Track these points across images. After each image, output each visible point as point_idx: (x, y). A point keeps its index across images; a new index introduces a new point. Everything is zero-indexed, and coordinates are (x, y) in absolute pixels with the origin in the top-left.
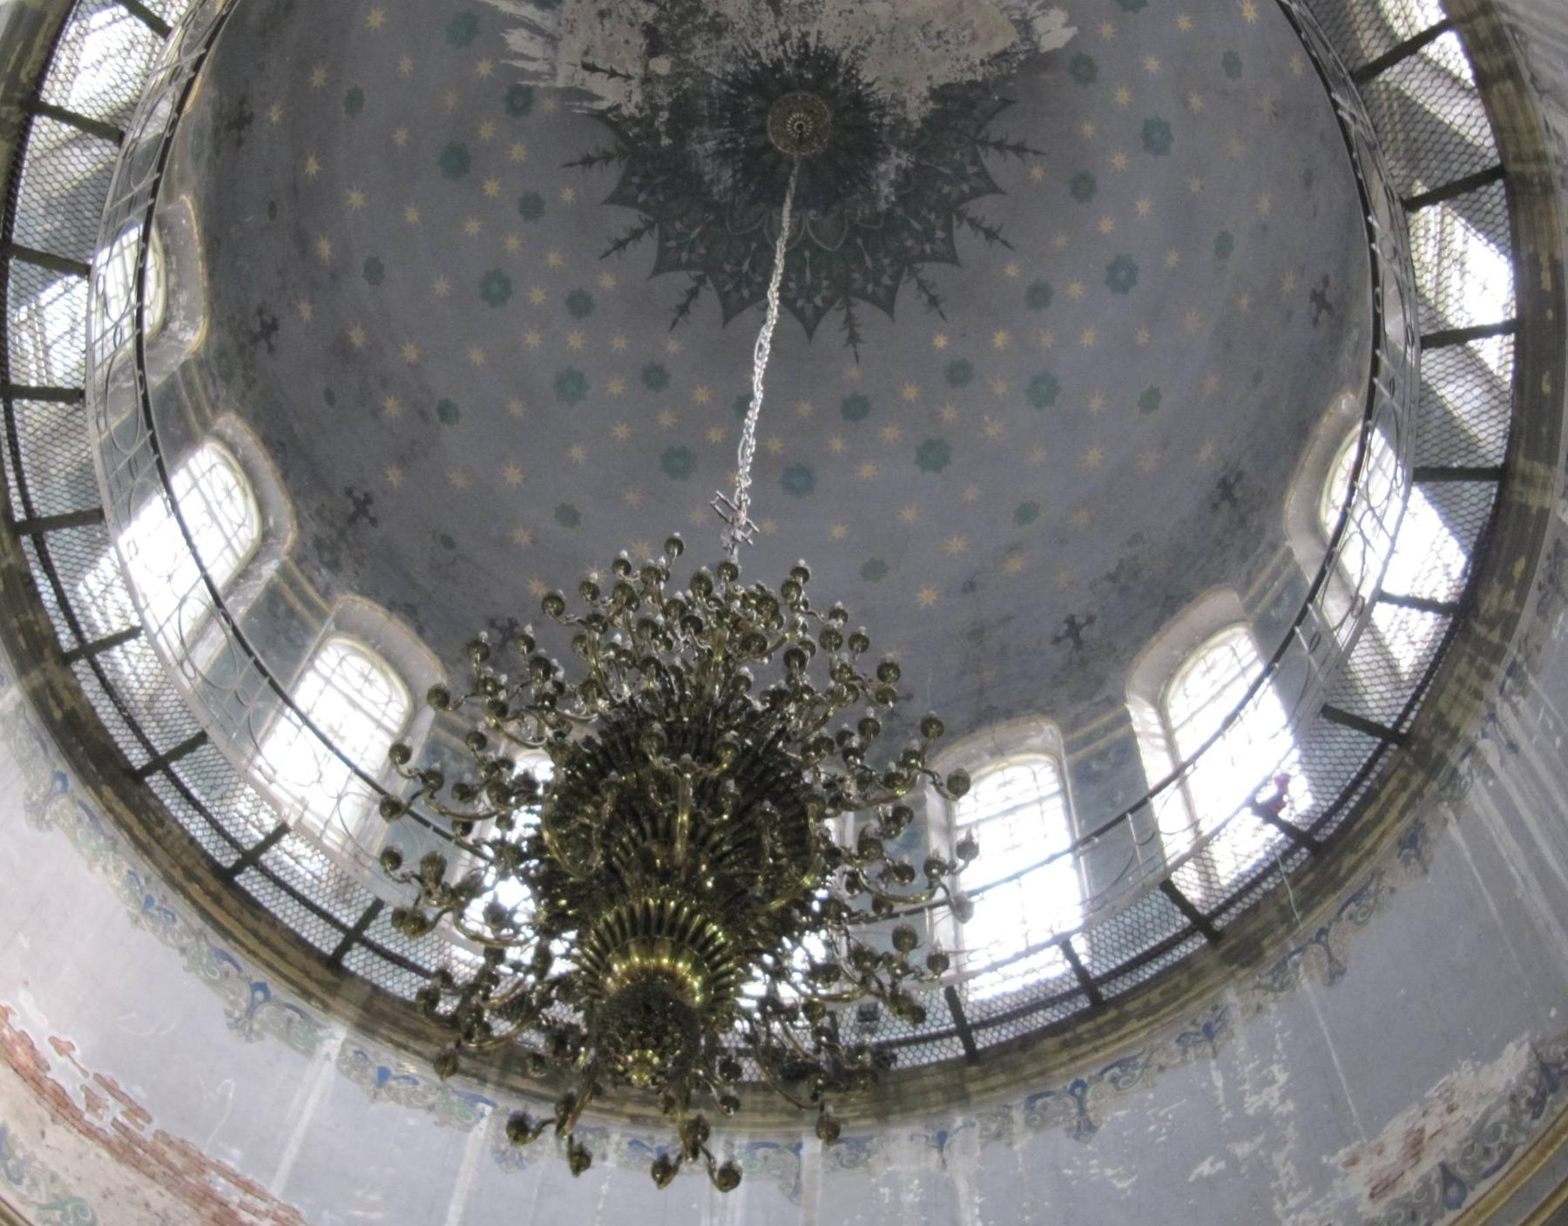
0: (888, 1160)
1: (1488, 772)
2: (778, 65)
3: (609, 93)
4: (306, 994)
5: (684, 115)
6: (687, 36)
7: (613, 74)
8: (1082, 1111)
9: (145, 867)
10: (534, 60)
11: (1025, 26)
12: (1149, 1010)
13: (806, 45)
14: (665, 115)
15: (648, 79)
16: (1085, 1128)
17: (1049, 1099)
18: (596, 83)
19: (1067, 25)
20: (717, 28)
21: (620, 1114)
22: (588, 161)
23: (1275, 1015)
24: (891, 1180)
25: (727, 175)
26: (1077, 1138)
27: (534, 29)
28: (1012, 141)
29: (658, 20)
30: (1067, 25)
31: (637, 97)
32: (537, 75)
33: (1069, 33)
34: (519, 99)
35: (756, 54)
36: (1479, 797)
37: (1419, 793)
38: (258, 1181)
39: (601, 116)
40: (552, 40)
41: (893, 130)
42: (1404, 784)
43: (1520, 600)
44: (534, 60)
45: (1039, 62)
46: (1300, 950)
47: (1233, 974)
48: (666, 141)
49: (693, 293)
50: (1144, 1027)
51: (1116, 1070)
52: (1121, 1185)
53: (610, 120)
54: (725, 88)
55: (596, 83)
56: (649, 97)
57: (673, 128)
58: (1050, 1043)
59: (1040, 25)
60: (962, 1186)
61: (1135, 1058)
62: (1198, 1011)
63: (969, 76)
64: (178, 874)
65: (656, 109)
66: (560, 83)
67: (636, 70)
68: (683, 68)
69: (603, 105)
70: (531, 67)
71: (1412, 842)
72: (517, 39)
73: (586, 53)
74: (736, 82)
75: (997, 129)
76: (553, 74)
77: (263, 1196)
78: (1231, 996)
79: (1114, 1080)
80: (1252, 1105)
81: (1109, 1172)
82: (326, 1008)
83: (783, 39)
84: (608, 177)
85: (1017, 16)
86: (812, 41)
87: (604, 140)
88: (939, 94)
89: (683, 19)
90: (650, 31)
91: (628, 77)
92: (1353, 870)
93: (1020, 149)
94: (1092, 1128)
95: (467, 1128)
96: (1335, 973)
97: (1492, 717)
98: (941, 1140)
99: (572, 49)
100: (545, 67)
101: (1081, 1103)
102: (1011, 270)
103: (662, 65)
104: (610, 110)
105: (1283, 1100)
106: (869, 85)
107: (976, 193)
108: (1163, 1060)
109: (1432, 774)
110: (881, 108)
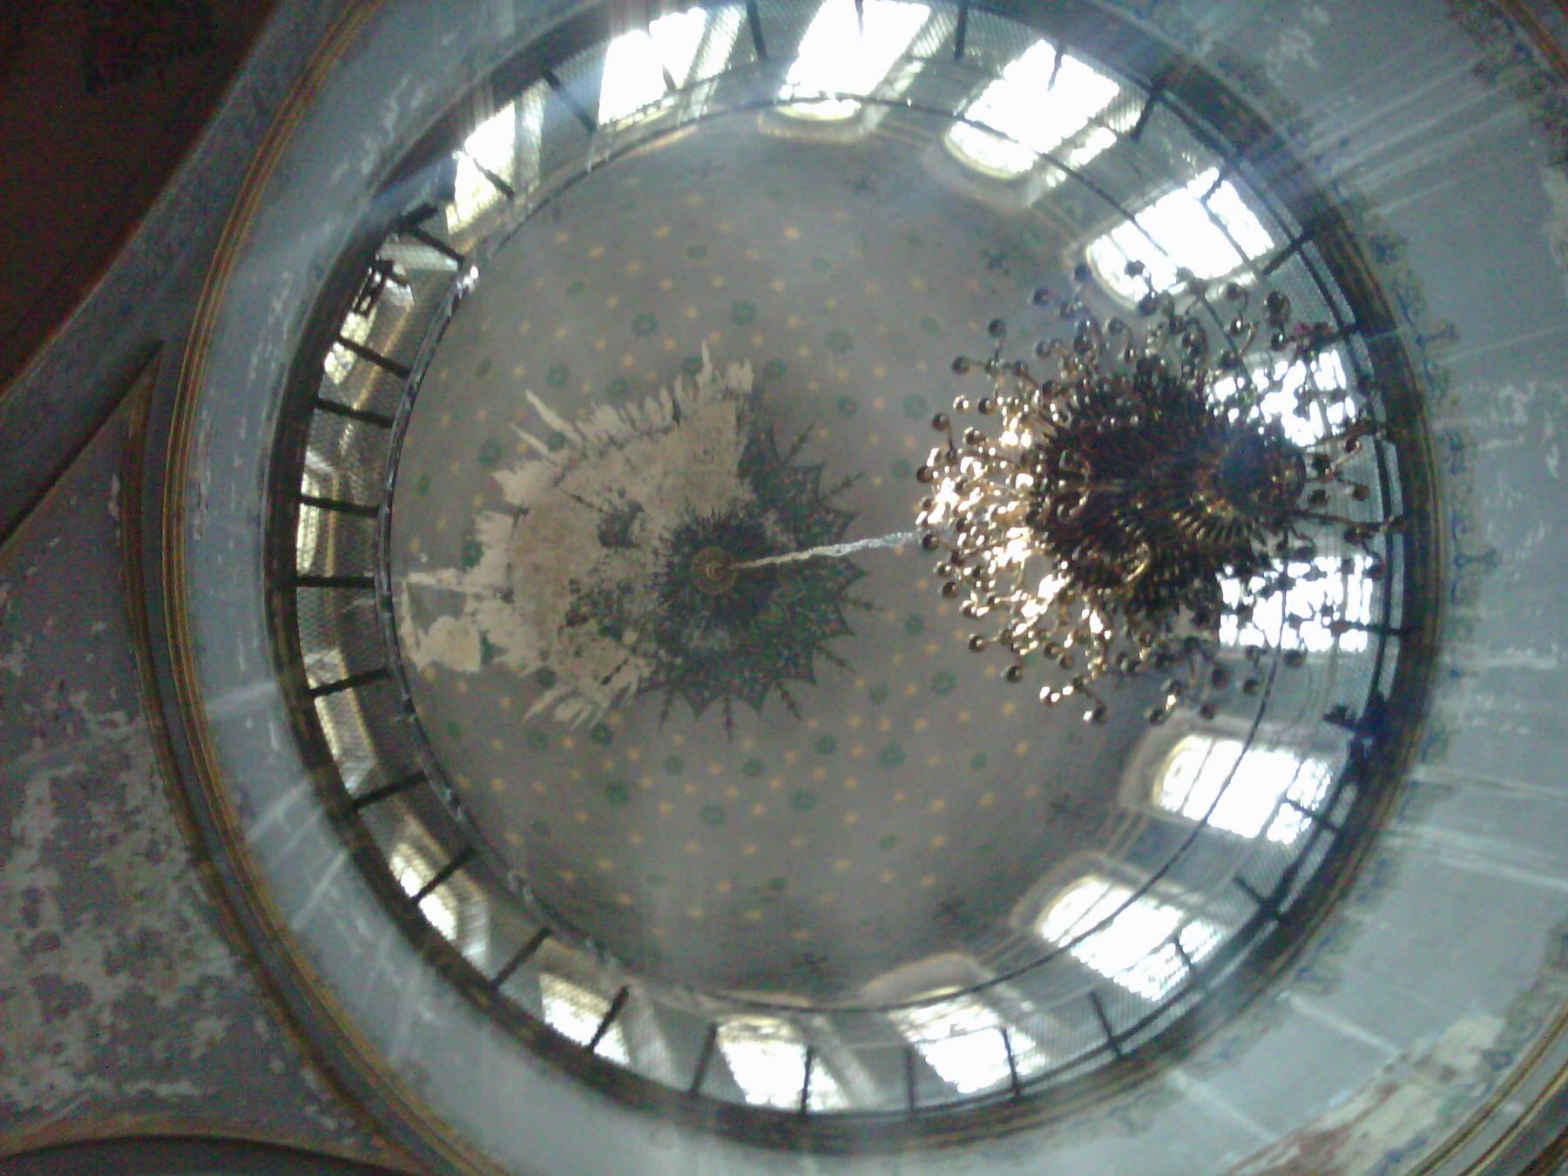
0: (1455, 717)
1: (1352, 173)
2: (670, 565)
3: (631, 677)
4: (1135, 1085)
5: (670, 641)
6: (620, 611)
7: (618, 669)
8: (1478, 559)
9: (982, 1146)
10: (579, 714)
11: (729, 394)
12: (1423, 492)
13: (668, 540)
14: (662, 653)
15: (634, 650)
16: (1490, 559)
17: (1459, 587)
18: (618, 682)
19: (742, 364)
20: (626, 589)
21: (1332, 906)
22: (665, 715)
23: (1462, 390)
24: (1469, 717)
25: (721, 634)
26: (1495, 565)
27: (562, 699)
28: (795, 439)
29: (600, 622)
30: (742, 364)
31: (641, 662)
32: (592, 716)
33: (748, 367)
34: (601, 734)
35: (656, 575)
36: (1368, 184)
37: (1350, 236)
38: (1257, 1148)
39: (640, 692)
40: (576, 693)
41: (750, 514)
42: (1339, 244)
43: (1247, 109)
44: (579, 714)
45: (755, 398)
46: (1425, 362)
47: (1424, 421)
48: (679, 661)
49: (785, 695)
50: (1435, 498)
51: (1458, 528)
52: (1542, 531)
53: (648, 686)
54: (666, 606)
55: (618, 682)
56: (645, 655)
57: (675, 653)
58: (1418, 572)
59: (733, 384)
60: (1497, 662)
61: (1454, 511)
62: (1441, 453)
63: (741, 449)
64: (1000, 1128)
65: (655, 655)
66: (605, 704)
67: (623, 654)
68: (640, 626)
69: (634, 688)
70: (584, 716)
71: (1384, 249)
72: (563, 713)
73: (596, 677)
74: (665, 597)
75: (783, 447)
76: (596, 705)
77: (1271, 1147)
78: (1438, 426)
79: (1464, 531)
80: (1520, 417)
81: (1529, 543)
82: (1150, 1076)
83: (656, 553)
84: (681, 708)
85: (720, 396)
86: (666, 535)
87: (659, 696)
88: (743, 472)
89: (609, 607)
90: (605, 631)
91: (626, 662)
92: (1384, 303)
93: (803, 438)
94: (1492, 553)
95: (1292, 1011)
96: (1451, 334)
97: (1318, 159)
98: (1456, 674)
99: (587, 684)
100: (590, 707)
101: (1470, 560)
102: (877, 481)
103: (630, 636)
104: (640, 684)
105: (1525, 391)
106: (713, 514)
107: (816, 481)
108: (1464, 488)
109: (1338, 220)
110: (731, 515)
